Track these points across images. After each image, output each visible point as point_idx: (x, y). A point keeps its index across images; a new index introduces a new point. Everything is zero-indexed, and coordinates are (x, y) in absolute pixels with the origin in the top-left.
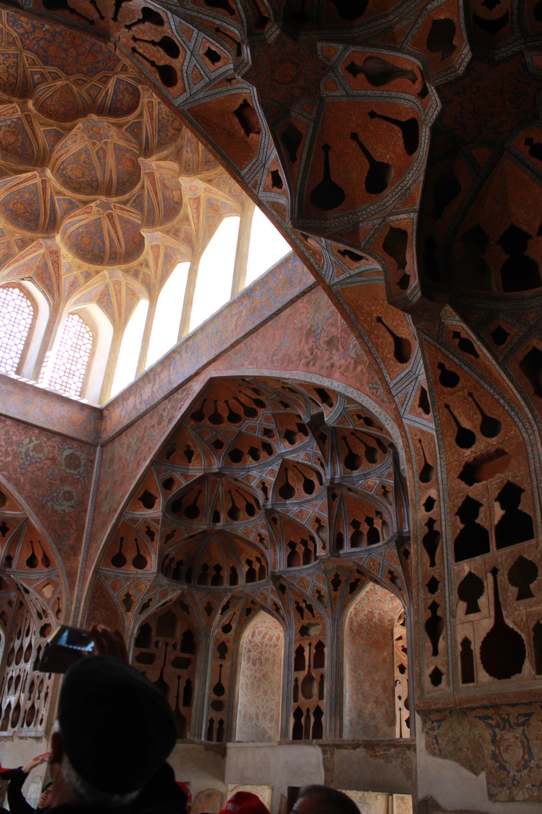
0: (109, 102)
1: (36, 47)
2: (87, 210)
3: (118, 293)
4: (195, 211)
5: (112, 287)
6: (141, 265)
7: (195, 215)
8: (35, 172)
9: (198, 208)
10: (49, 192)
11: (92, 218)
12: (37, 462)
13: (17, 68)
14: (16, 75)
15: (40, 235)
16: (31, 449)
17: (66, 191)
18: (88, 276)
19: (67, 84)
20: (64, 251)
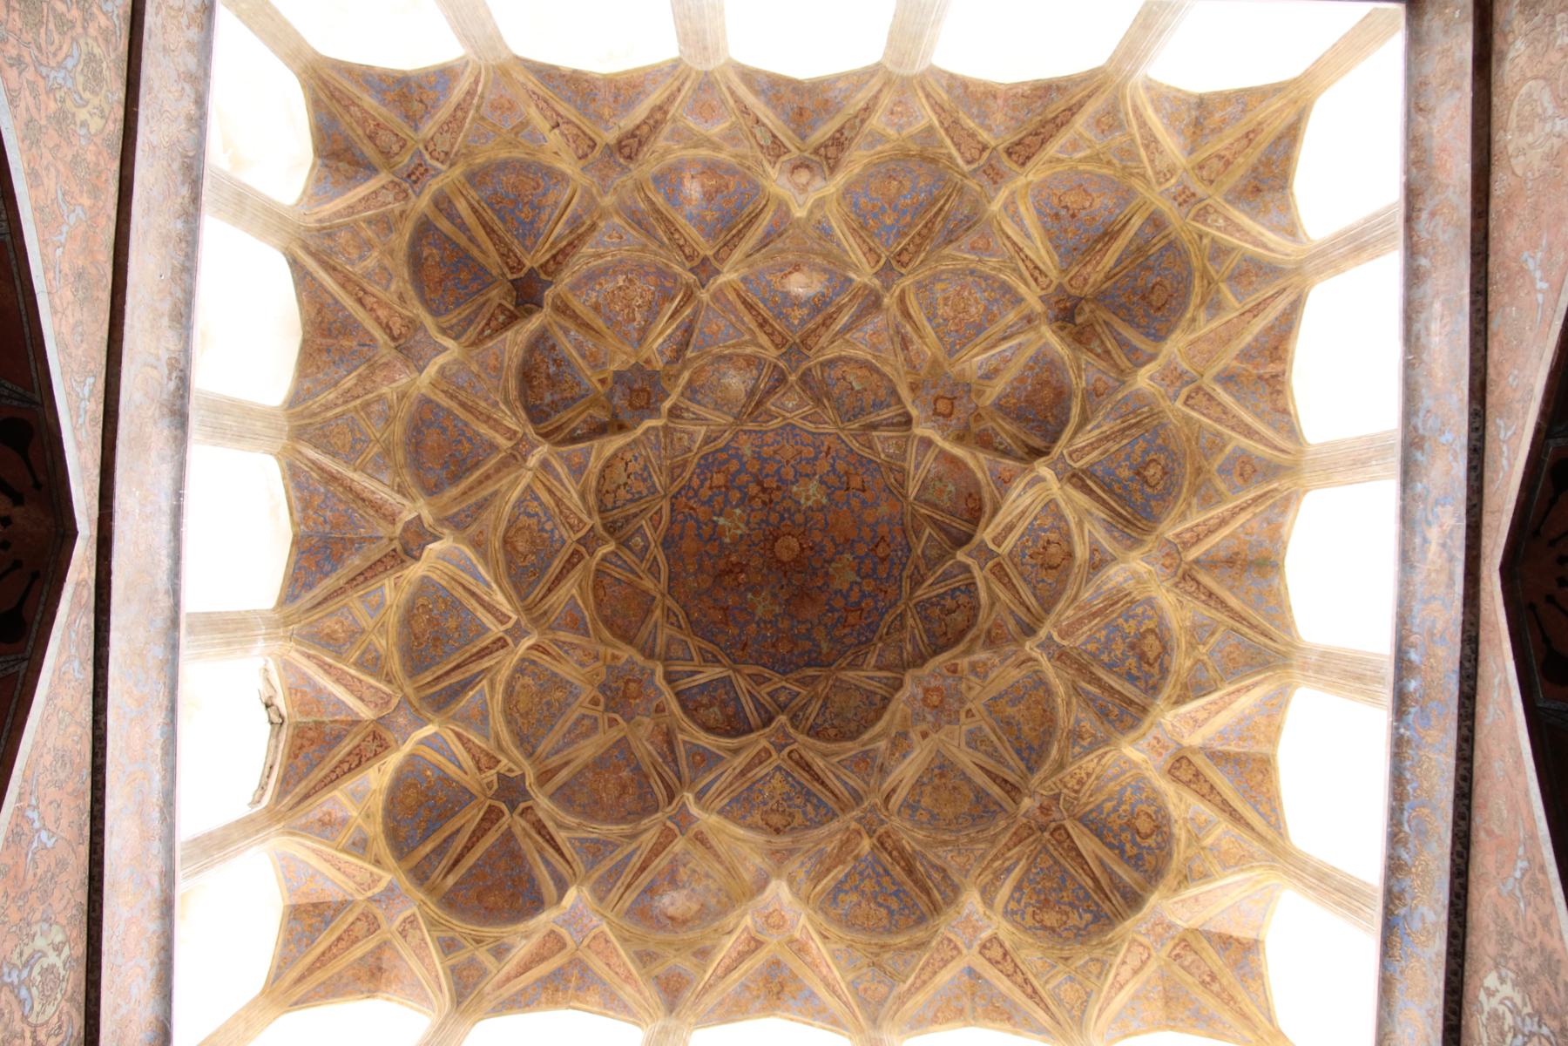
0: (684, 684)
1: (680, 517)
2: (484, 760)
3: (348, 939)
4: (734, 955)
5: (351, 919)
6: (478, 941)
7: (727, 961)
8: (515, 617)
9: (742, 957)
10: (486, 663)
11: (470, 778)
12: (22, 1002)
13: (632, 501)
14: (619, 503)
15: (409, 690)
16: (45, 962)
17: (499, 697)
18: (360, 846)
19: (654, 598)
20: (393, 761)
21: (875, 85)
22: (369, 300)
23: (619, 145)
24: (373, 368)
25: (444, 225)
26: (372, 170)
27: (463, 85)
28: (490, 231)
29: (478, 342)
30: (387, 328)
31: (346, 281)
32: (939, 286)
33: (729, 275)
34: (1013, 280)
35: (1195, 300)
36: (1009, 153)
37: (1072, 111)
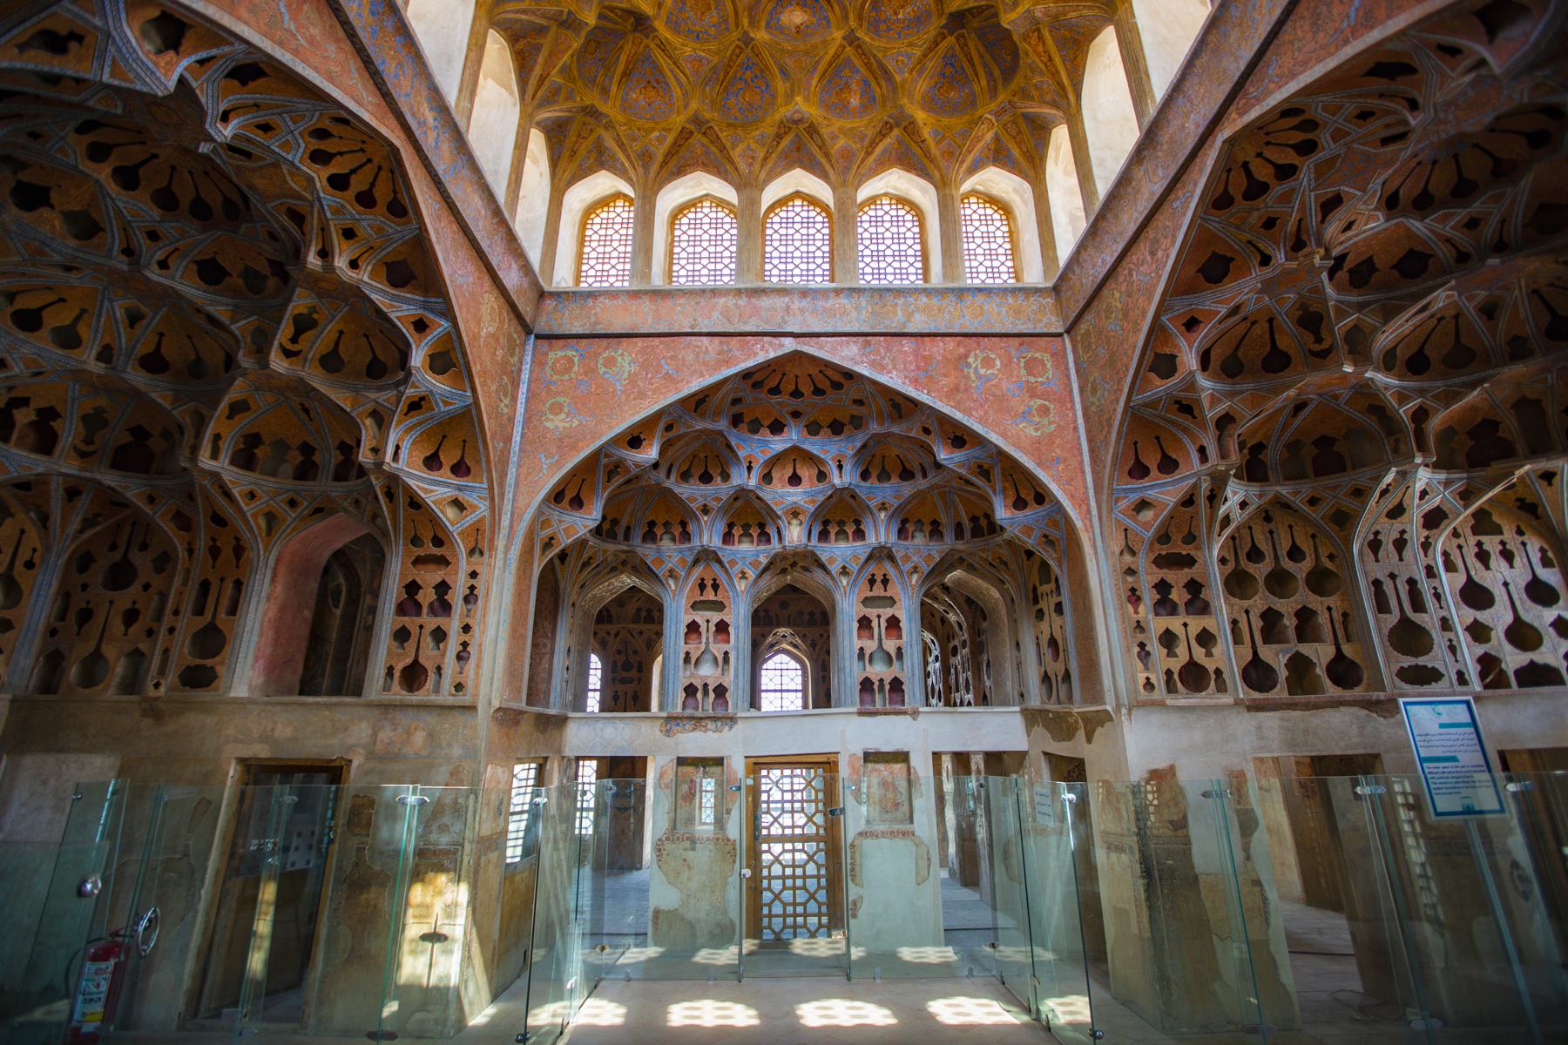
21: (762, 176)
22: (1045, 59)
23: (891, 129)
24: (1056, 17)
25: (997, 73)
26: (1025, 116)
27: (965, 165)
28: (970, 61)
29: (989, 7)
30: (1041, 38)
31: (1055, 74)
32: (715, 20)
33: (838, 35)
34: (675, 40)
35: (574, 65)
36: (691, 133)
37: (665, 163)
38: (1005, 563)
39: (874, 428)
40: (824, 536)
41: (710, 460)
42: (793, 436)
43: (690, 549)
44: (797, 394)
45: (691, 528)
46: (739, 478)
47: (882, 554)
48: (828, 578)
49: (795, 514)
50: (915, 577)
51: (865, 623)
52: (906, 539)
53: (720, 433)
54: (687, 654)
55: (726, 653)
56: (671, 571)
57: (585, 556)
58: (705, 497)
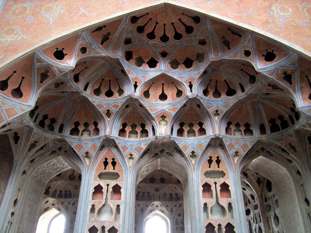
38: (293, 148)
39: (212, 57)
40: (180, 132)
41: (112, 80)
42: (163, 67)
43: (99, 139)
44: (165, 38)
45: (100, 126)
46: (129, 91)
47: (217, 143)
48: (183, 159)
49: (163, 117)
50: (236, 159)
51: (207, 187)
52: (231, 134)
53: (117, 62)
54: (93, 206)
55: (118, 206)
56: (87, 153)
57: (32, 140)
58: (108, 104)
